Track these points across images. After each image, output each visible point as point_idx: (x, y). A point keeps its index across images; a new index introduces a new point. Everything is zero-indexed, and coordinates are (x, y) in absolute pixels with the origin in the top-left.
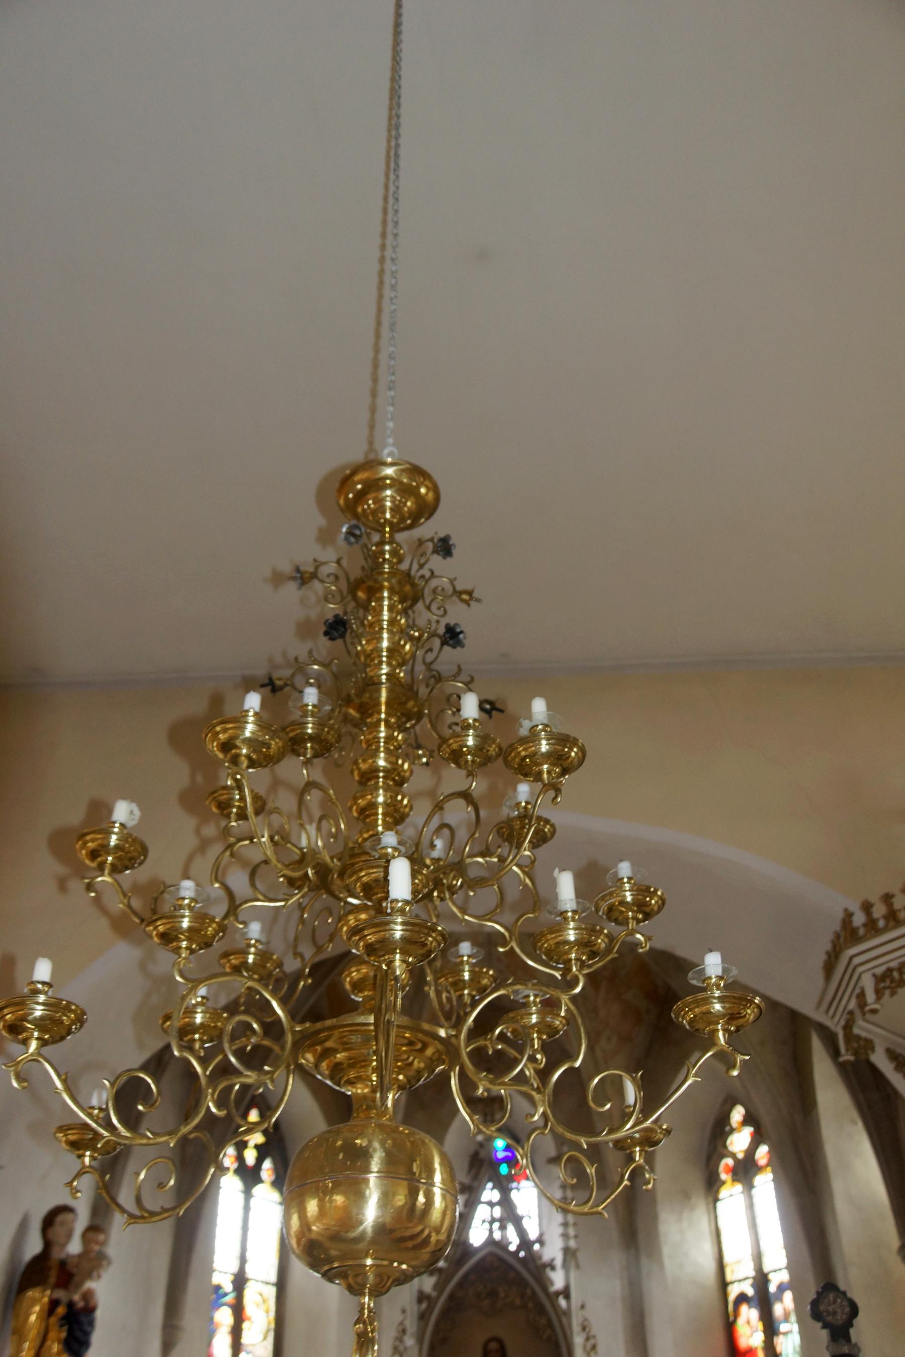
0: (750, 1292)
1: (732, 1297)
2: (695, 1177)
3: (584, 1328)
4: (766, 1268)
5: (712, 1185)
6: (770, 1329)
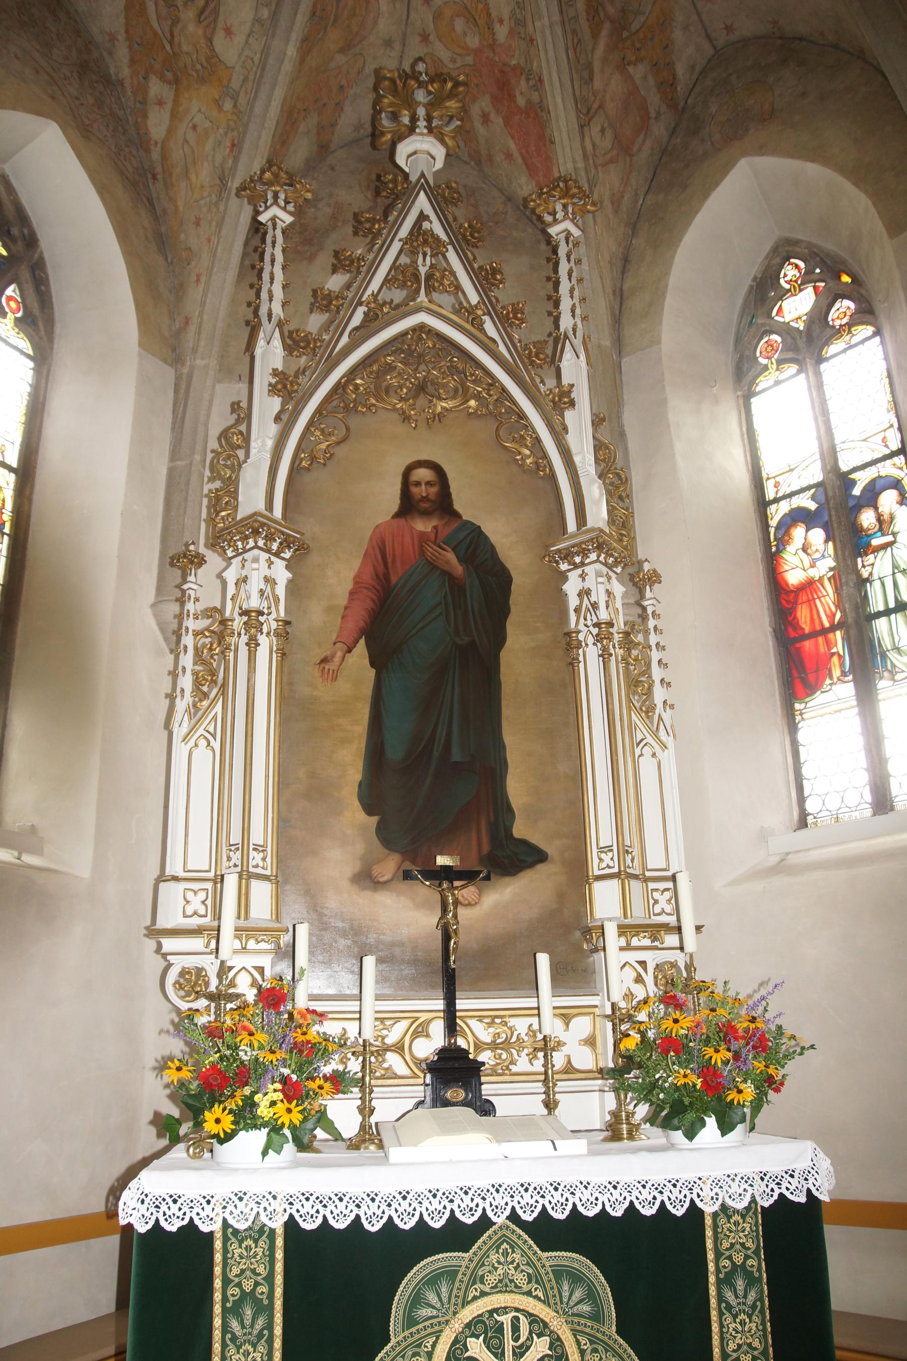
1: (773, 523)
2: (722, 359)
5: (743, 375)
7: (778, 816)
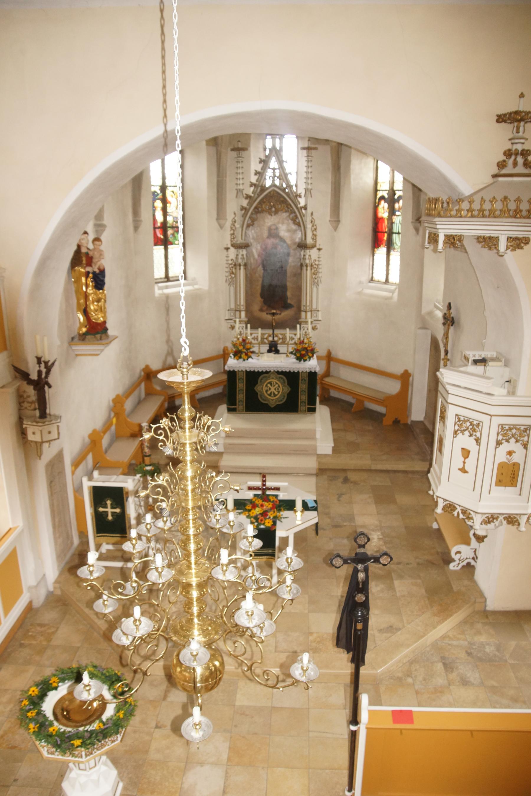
0: (386, 196)
1: (378, 196)
3: (312, 222)
4: (395, 189)
6: (392, 212)
7: (365, 278)
